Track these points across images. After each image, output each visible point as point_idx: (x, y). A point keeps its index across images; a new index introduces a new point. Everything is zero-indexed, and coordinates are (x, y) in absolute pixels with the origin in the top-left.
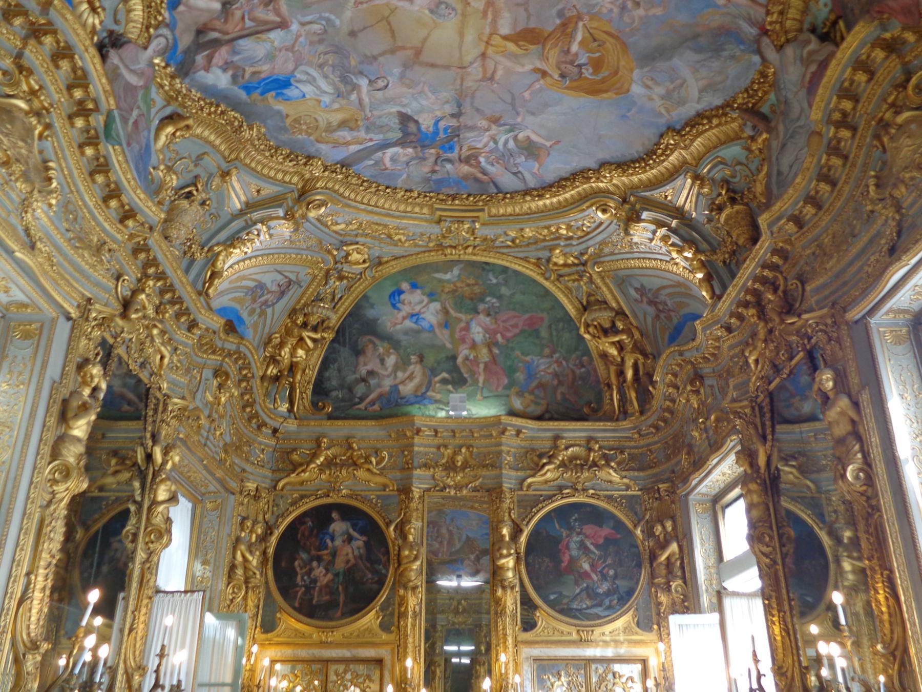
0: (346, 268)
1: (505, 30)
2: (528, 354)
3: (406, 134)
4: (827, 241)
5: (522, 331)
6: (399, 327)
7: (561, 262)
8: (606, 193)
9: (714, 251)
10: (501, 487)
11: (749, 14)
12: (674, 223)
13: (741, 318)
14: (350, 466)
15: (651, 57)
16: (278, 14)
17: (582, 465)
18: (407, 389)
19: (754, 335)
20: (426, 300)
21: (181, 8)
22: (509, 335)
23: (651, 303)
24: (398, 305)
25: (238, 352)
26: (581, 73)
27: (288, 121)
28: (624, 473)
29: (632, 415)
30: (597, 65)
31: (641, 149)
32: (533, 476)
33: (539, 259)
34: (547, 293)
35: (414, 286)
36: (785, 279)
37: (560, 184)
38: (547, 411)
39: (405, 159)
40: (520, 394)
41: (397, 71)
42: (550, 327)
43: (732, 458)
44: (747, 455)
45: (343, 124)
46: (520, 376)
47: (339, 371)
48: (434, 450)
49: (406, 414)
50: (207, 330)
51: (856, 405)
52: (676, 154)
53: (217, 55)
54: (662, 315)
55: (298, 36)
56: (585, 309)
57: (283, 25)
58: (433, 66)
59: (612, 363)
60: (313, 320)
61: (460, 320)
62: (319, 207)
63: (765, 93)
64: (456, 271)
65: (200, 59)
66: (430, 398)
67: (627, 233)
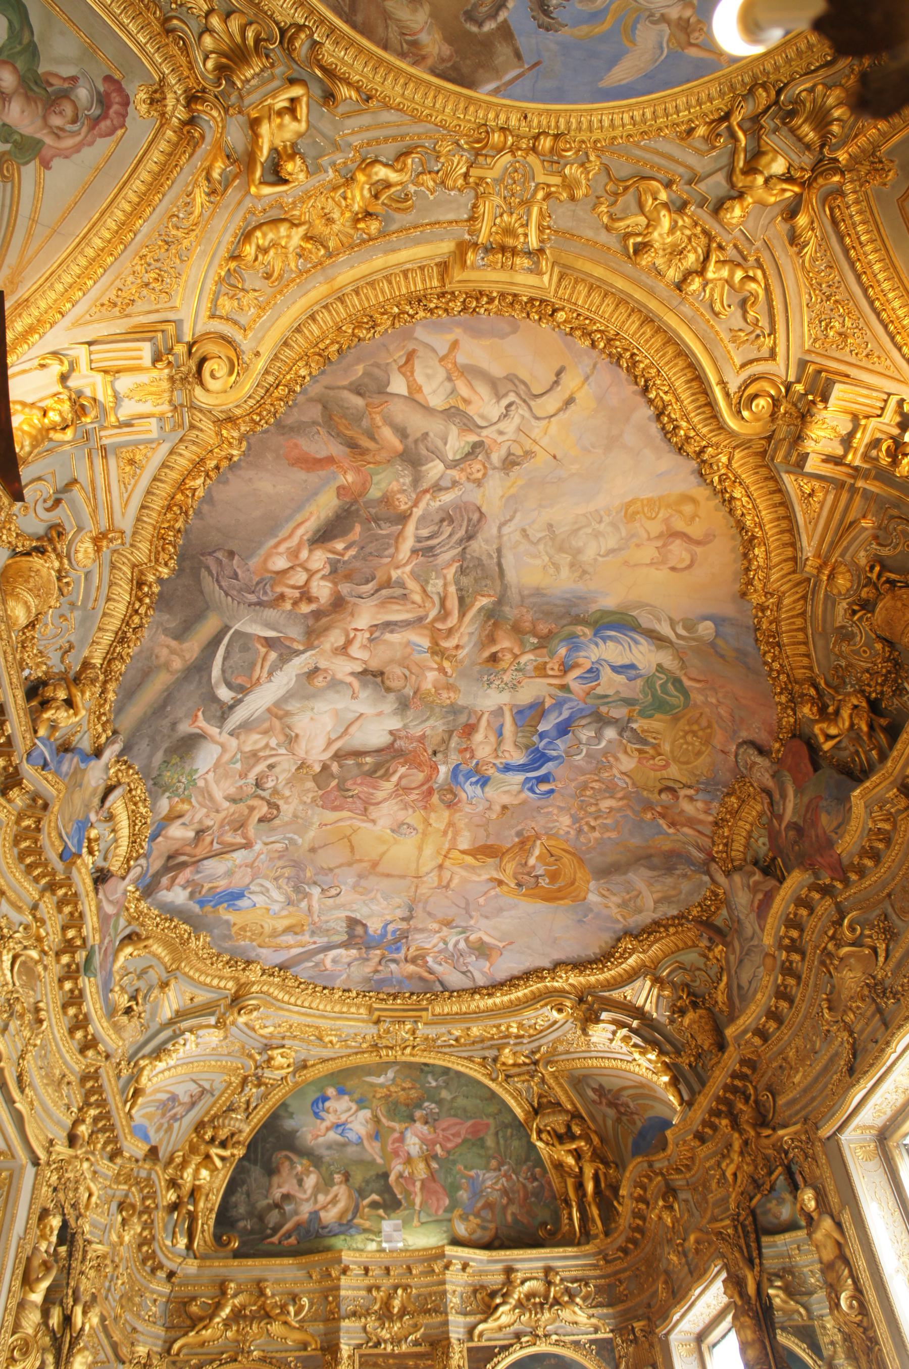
0: (267, 1073)
1: (464, 845)
2: (472, 1168)
3: (351, 936)
4: (791, 1054)
5: (465, 1141)
6: (321, 1140)
7: (511, 1062)
8: (561, 992)
9: (678, 1053)
10: (448, 1338)
12: (635, 1024)
13: (715, 1128)
14: (261, 1319)
15: (605, 872)
16: (245, 838)
17: (542, 1304)
18: (329, 1216)
19: (729, 1146)
20: (354, 1107)
21: (160, 839)
22: (450, 1145)
23: (611, 1104)
24: (322, 1114)
25: (148, 1178)
26: (537, 883)
27: (234, 930)
28: (591, 1311)
29: (596, 1236)
30: (554, 876)
31: (597, 951)
32: (485, 1321)
33: (484, 1058)
34: (493, 1095)
35: (341, 1092)
36: (755, 1088)
37: (512, 982)
38: (496, 1237)
39: (348, 960)
40: (464, 1218)
41: (351, 881)
42: (497, 1134)
43: (718, 1287)
44: (735, 1283)
45: (288, 930)
46: (463, 1195)
47: (248, 1195)
48: (363, 1293)
49: (328, 1249)
50: (130, 1159)
51: (839, 1225)
52: (634, 957)
54: (624, 1118)
55: (259, 854)
56: (536, 1112)
57: (248, 845)
58: (388, 876)
59: (569, 1175)
60: (223, 1134)
61: (393, 1130)
62: (251, 1011)
63: (718, 908)
64: (391, 1074)
66: (357, 1227)
67: (584, 1032)
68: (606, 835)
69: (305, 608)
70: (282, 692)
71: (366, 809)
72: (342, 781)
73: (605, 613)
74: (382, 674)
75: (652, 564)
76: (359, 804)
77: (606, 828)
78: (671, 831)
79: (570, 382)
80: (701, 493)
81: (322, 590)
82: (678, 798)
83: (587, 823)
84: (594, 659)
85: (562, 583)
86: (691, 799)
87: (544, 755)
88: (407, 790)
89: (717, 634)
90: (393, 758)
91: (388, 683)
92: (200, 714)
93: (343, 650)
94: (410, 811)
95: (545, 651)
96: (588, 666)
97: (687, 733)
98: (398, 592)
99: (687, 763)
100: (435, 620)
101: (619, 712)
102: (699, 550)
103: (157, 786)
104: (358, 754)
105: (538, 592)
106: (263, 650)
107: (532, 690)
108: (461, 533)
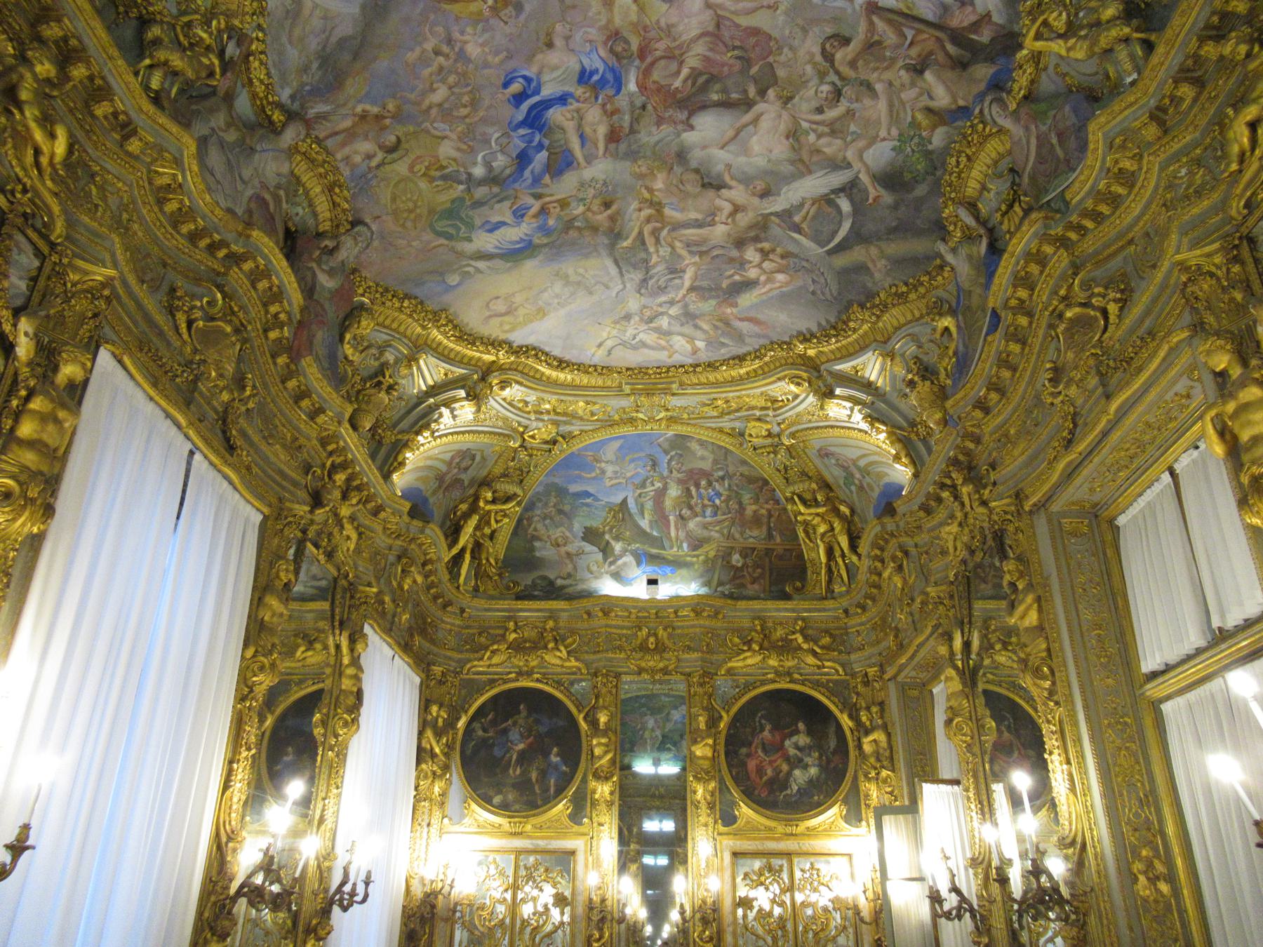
11: (329, 121)
16: (871, 23)
21: (961, 103)
53: (965, 24)
65: (984, 37)
68: (418, 51)
69: (766, 245)
70: (796, 184)
71: (718, 26)
72: (744, 71)
73: (531, 256)
74: (703, 186)
75: (513, 294)
76: (726, 34)
77: (424, 61)
78: (359, 109)
79: (601, 353)
80: (502, 337)
81: (751, 254)
82: (380, 147)
83: (447, 56)
84: (524, 225)
85: (571, 267)
86: (369, 157)
87: (531, 127)
88: (669, 56)
89: (444, 281)
90: (688, 98)
91: (698, 177)
92: (871, 201)
93: (737, 209)
94: (663, 24)
95: (566, 219)
96: (525, 219)
97: (416, 207)
98: (694, 249)
99: (396, 185)
100: (662, 228)
101: (481, 192)
102: (488, 313)
103: (936, 162)
104: (726, 105)
105: (587, 256)
106: (804, 226)
107: (567, 185)
108: (650, 283)
